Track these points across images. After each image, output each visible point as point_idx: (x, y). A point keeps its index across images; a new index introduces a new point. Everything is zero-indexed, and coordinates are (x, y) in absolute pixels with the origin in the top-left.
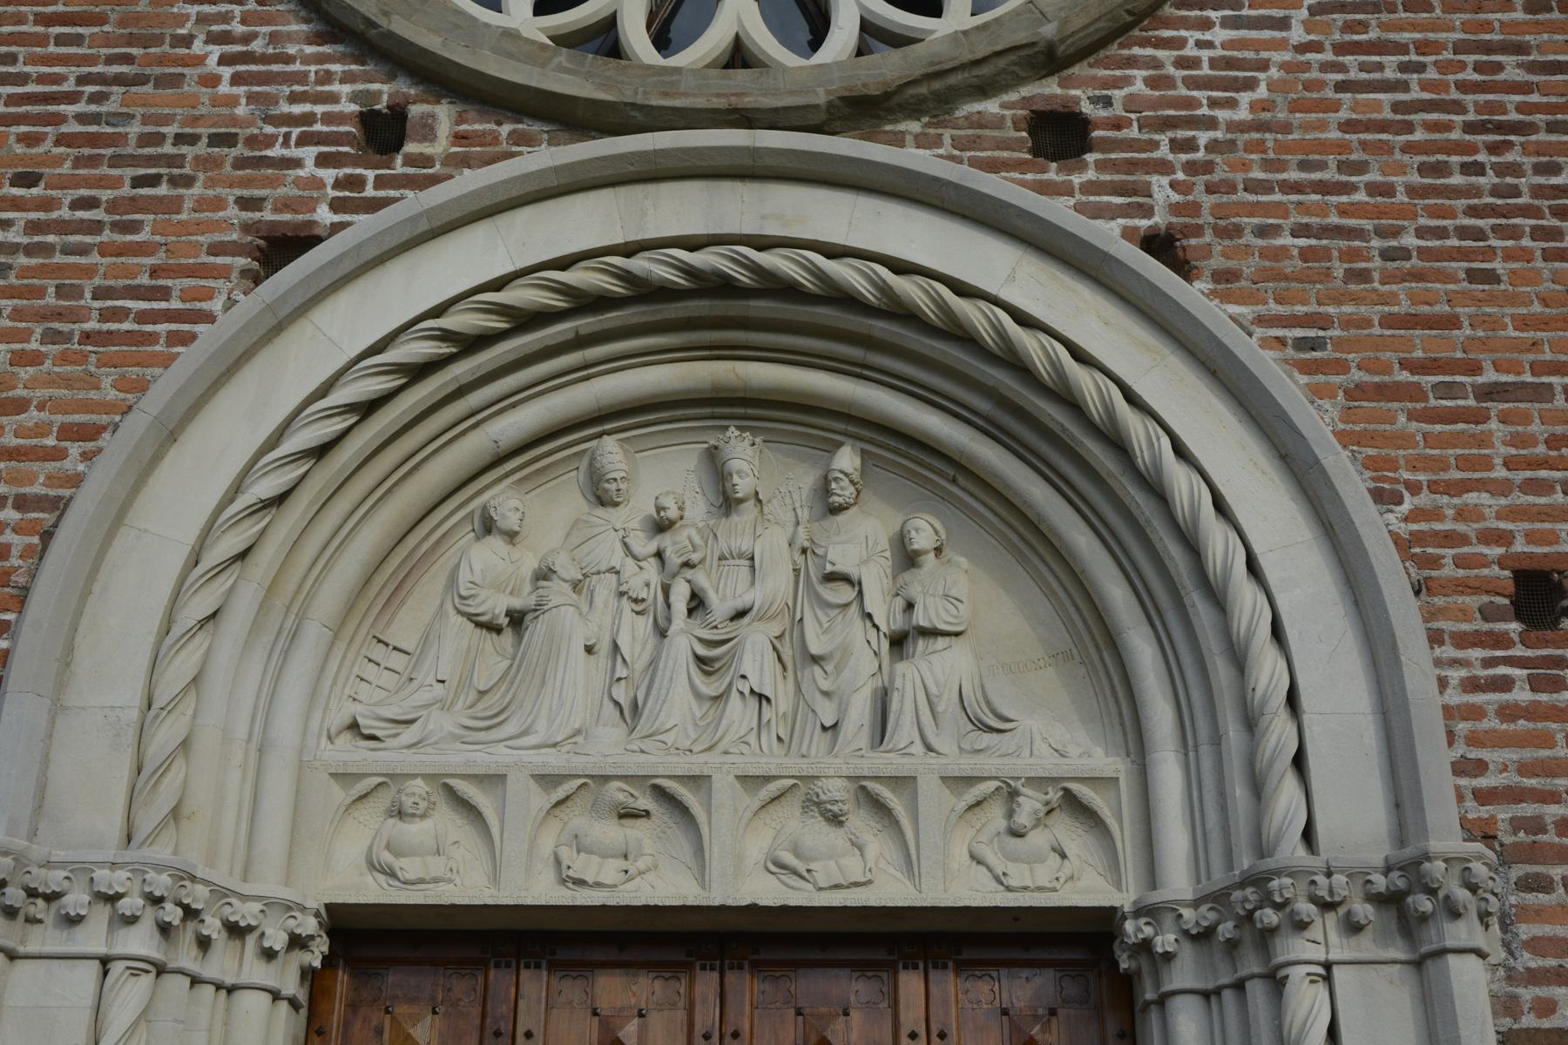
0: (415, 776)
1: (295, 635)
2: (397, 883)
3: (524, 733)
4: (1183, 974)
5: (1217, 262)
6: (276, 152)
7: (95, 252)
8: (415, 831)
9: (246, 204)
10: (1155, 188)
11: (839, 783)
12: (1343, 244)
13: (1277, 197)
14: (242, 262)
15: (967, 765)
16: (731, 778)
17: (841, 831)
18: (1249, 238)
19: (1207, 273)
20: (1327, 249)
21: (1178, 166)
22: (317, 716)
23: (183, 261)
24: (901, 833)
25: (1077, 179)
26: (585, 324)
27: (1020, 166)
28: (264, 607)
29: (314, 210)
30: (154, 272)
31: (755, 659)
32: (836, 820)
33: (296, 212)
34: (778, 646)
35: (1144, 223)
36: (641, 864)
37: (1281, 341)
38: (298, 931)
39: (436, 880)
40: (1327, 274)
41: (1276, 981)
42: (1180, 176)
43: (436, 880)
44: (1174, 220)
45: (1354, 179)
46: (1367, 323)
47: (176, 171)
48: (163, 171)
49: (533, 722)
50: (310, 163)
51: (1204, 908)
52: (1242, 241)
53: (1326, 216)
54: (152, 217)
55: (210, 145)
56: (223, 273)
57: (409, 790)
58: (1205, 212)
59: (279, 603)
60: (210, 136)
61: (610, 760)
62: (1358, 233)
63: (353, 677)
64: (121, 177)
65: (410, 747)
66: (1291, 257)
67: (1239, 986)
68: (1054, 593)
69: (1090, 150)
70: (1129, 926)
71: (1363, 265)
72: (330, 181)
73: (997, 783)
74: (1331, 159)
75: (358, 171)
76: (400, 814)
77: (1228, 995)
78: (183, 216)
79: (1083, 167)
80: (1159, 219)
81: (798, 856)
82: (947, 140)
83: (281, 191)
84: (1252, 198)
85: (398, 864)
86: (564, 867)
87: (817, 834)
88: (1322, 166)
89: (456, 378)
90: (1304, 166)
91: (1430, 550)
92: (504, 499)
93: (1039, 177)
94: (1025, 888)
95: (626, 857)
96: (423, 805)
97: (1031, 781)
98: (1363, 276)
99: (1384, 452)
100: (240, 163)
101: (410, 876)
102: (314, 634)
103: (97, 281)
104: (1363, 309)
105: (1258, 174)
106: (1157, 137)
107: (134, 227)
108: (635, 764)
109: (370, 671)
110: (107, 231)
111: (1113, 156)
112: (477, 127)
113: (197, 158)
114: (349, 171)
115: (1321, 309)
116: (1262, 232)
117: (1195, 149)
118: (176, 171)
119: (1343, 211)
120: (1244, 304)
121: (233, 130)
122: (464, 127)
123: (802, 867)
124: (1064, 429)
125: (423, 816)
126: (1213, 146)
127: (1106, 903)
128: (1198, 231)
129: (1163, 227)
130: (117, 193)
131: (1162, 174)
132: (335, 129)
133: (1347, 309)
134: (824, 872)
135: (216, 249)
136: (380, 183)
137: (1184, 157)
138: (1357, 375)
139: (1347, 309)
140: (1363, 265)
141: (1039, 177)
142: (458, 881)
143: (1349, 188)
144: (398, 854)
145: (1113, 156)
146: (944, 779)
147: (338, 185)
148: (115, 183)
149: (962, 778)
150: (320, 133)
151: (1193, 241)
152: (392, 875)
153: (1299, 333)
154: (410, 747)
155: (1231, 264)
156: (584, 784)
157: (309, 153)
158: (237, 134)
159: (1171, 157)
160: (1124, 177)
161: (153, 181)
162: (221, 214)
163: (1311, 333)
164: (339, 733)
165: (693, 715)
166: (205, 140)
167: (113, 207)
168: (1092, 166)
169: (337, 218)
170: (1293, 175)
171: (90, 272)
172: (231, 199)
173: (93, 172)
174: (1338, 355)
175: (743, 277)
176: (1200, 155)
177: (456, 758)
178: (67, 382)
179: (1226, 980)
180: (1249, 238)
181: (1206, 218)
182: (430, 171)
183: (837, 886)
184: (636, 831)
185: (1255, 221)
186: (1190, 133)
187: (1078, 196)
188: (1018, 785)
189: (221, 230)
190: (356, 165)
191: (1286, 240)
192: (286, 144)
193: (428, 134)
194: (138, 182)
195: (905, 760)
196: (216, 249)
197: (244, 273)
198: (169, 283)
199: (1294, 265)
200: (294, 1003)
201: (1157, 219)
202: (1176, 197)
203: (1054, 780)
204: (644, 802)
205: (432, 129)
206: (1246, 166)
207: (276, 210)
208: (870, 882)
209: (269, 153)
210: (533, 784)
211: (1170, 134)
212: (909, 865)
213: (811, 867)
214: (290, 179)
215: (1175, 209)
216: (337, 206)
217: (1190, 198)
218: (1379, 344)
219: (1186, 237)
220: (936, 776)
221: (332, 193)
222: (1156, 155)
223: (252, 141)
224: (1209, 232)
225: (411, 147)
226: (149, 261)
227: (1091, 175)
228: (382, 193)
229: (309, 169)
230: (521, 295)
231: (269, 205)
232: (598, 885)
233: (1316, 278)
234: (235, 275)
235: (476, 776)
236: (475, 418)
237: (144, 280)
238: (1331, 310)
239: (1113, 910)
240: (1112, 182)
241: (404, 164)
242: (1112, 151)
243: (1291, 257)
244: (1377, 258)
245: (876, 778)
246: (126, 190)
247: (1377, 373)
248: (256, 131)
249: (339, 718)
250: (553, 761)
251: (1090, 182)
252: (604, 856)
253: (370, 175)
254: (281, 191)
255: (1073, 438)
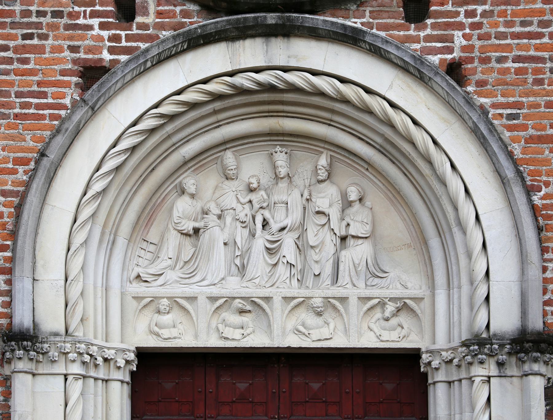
0: (164, 298)
1: (114, 242)
2: (161, 339)
3: (203, 280)
4: (440, 376)
5: (479, 76)
6: (81, 21)
7: (12, 74)
8: (166, 319)
9: (74, 49)
10: (456, 38)
11: (320, 300)
12: (534, 65)
13: (509, 41)
14: (75, 79)
15: (368, 293)
16: (280, 297)
17: (321, 318)
18: (494, 64)
19: (474, 82)
20: (527, 69)
21: (467, 25)
22: (125, 273)
23: (50, 79)
24: (344, 320)
25: (422, 34)
26: (218, 105)
27: (398, 27)
28: (103, 233)
29: (101, 53)
30: (39, 84)
31: (289, 250)
32: (319, 314)
33: (94, 54)
34: (297, 242)
35: (449, 57)
36: (249, 331)
37: (501, 115)
38: (128, 359)
39: (175, 338)
40: (525, 81)
41: (471, 380)
42: (467, 31)
43: (175, 338)
44: (462, 55)
45: (544, 30)
46: (538, 106)
47: (40, 31)
48: (34, 31)
49: (206, 275)
50: (96, 27)
51: (450, 352)
52: (490, 65)
53: (529, 51)
54: (33, 56)
55: (52, 17)
56: (67, 85)
57: (162, 303)
58: (476, 50)
59: (108, 231)
60: (52, 12)
61: (235, 291)
62: (541, 60)
63: (136, 256)
64: (16, 34)
65: (161, 286)
66: (510, 73)
67: (460, 380)
68: (405, 220)
69: (429, 18)
70: (424, 356)
71: (541, 76)
72: (106, 38)
73: (379, 300)
74: (535, 20)
75: (118, 32)
76: (159, 312)
77: (456, 383)
78: (47, 55)
79: (425, 27)
80: (456, 54)
81: (305, 328)
82: (367, 14)
83: (87, 42)
84: (497, 42)
85: (161, 332)
86: (220, 332)
87: (311, 320)
88: (530, 24)
89: (167, 132)
90: (523, 24)
91: (549, 212)
92: (190, 182)
93: (406, 33)
94: (388, 341)
95: (242, 328)
96: (168, 309)
97: (391, 299)
98: (540, 82)
99: (537, 168)
100: (68, 27)
101: (166, 337)
102: (121, 242)
103: (16, 89)
104: (538, 99)
105: (502, 29)
106: (459, 9)
107: (25, 61)
108: (245, 292)
109: (144, 245)
110: (15, 63)
111: (439, 21)
112: (166, 8)
113: (48, 24)
114: (113, 32)
115: (520, 99)
116: (500, 60)
117: (476, 16)
118: (40, 31)
119: (537, 48)
120: (488, 97)
121: (61, 9)
122: (160, 8)
123: (306, 333)
124: (410, 155)
125: (168, 313)
126: (484, 14)
127: (417, 347)
128: (471, 60)
129: (457, 59)
130: (16, 43)
131: (459, 30)
132: (105, 8)
133: (531, 99)
134: (315, 334)
135: (63, 73)
136: (129, 38)
137: (470, 20)
138: (531, 132)
139: (531, 99)
140: (541, 76)
141: (406, 33)
142: (183, 338)
143: (540, 35)
144: (161, 328)
145: (439, 21)
146: (359, 298)
147: (110, 39)
148: (13, 38)
149: (366, 298)
150: (99, 11)
151: (469, 66)
152: (158, 335)
153: (509, 111)
154: (161, 286)
155: (484, 77)
156: (227, 300)
157: (95, 22)
158: (63, 11)
159: (464, 21)
160: (443, 32)
161: (29, 36)
162: (63, 54)
163: (514, 111)
164: (134, 280)
165: (266, 271)
166: (49, 14)
167: (16, 50)
168: (429, 27)
169: (112, 57)
170: (517, 29)
171: (11, 84)
172: (66, 47)
173: (4, 31)
174: (524, 122)
175: (281, 85)
176: (477, 19)
177: (179, 290)
178: (12, 138)
179: (455, 378)
180: (494, 64)
181: (477, 53)
182: (148, 32)
183: (320, 340)
184: (245, 319)
185: (497, 54)
186: (474, 7)
187: (422, 43)
188: (387, 300)
189: (64, 63)
190: (117, 29)
191: (509, 64)
192: (85, 17)
193: (146, 13)
194: (25, 37)
195: (345, 291)
196: (63, 73)
197: (77, 85)
198: (46, 89)
199: (509, 78)
200: (128, 383)
201: (455, 54)
202: (464, 43)
203: (400, 299)
204: (248, 308)
205: (147, 9)
206: (496, 25)
207: (86, 53)
208: (331, 338)
209: (78, 22)
210: (207, 300)
211: (465, 8)
212: (346, 331)
213: (310, 332)
214: (89, 36)
215: (464, 49)
216: (111, 50)
217: (470, 42)
218: (543, 116)
219: (466, 63)
220: (356, 297)
221: (109, 44)
222: (458, 19)
223: (71, 15)
224: (476, 61)
225: (139, 19)
226: (36, 78)
227: (428, 31)
228: (129, 44)
229: (96, 31)
230: (190, 96)
231: (82, 50)
232: (233, 339)
233: (520, 83)
234: (73, 86)
235: (186, 297)
236: (176, 147)
237: (35, 88)
238: (524, 99)
239: (419, 349)
240: (437, 35)
241: (137, 29)
242: (438, 18)
243: (510, 73)
244: (548, 73)
245: (334, 298)
246: (20, 42)
247: (540, 131)
248: (71, 10)
249: (134, 274)
250: (215, 291)
251: (428, 35)
252: (235, 328)
253: (123, 33)
254: (87, 42)
255: (413, 158)
